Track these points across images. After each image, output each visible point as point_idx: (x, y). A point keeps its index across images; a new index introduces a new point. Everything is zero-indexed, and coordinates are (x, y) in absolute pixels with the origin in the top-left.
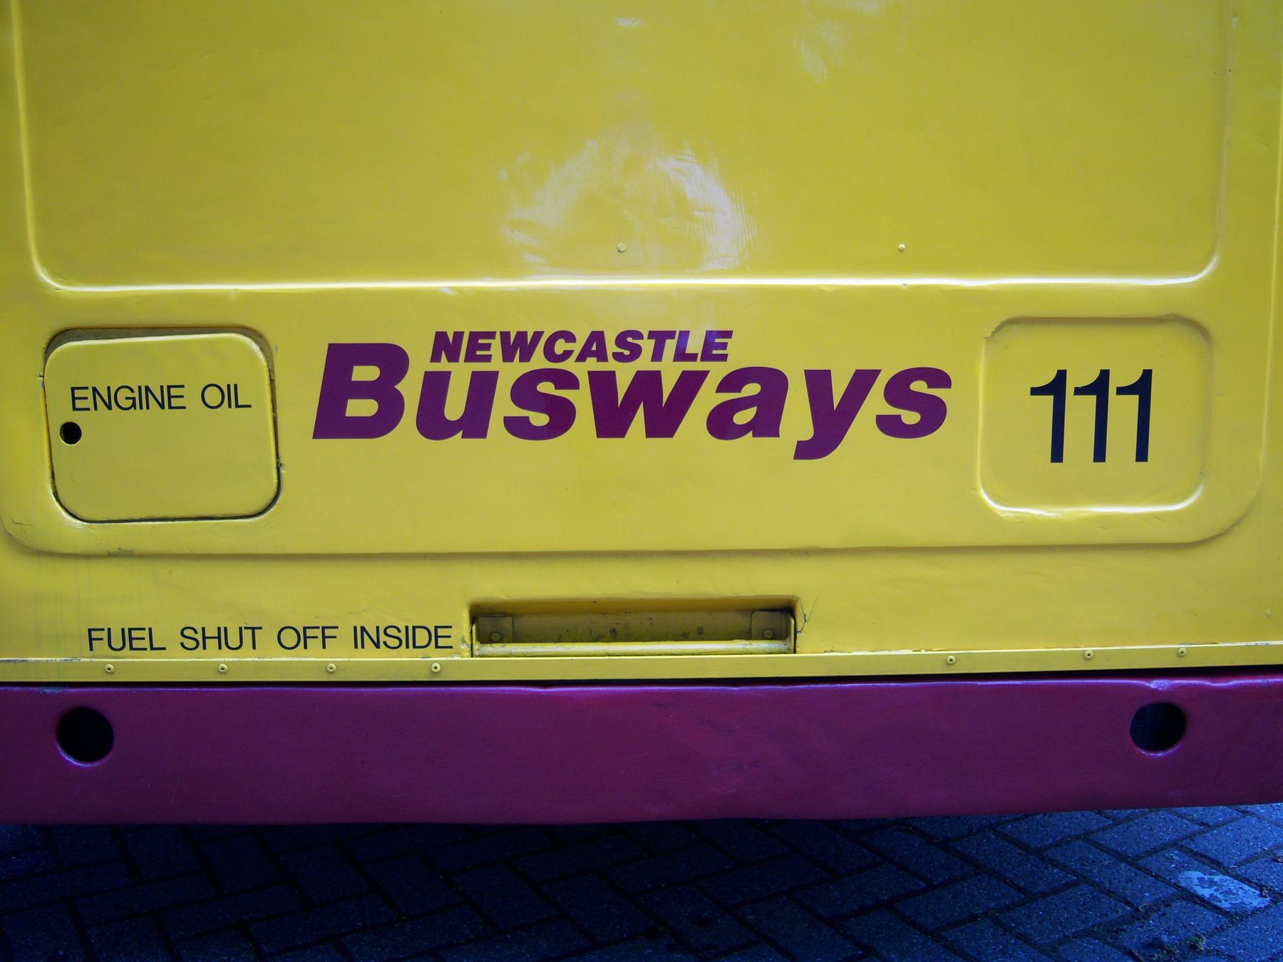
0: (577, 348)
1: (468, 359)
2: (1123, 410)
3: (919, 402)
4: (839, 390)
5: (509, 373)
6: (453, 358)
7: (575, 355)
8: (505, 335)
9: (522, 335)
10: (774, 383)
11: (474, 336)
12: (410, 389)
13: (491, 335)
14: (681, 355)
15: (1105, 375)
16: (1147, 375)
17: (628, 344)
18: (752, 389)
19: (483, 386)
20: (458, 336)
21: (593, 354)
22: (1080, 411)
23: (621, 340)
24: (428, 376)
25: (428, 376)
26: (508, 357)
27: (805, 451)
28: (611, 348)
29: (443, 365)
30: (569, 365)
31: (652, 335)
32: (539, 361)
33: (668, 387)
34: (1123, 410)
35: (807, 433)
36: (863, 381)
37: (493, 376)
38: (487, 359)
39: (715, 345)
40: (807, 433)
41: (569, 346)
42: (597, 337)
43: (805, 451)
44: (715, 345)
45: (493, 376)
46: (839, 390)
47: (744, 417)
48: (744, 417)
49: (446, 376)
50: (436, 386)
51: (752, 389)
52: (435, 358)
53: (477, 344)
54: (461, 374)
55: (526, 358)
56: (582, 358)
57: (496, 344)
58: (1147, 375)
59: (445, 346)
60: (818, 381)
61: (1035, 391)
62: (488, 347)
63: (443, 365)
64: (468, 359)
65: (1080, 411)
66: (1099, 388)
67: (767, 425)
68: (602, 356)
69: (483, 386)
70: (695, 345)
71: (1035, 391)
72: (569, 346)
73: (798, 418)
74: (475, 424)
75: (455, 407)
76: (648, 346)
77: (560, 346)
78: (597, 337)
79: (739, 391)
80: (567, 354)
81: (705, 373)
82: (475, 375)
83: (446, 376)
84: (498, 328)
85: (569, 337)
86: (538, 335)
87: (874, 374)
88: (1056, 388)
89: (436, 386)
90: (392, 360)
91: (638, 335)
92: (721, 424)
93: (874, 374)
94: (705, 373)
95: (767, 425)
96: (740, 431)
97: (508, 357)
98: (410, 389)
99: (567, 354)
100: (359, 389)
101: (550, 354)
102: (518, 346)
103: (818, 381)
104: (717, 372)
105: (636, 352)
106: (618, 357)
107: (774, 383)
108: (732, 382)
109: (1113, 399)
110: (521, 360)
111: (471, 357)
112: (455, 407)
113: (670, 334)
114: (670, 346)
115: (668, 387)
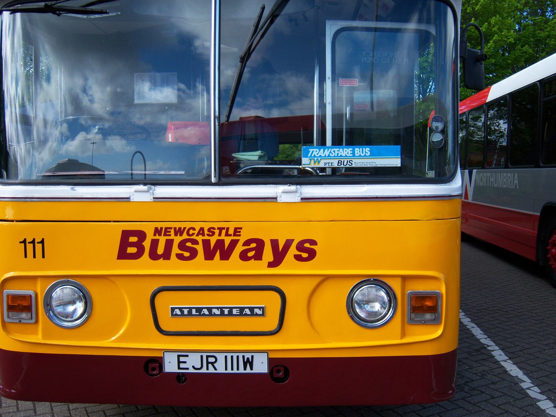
0: (196, 232)
1: (164, 235)
2: (39, 247)
5: (177, 240)
6: (160, 235)
7: (195, 235)
8: (175, 228)
9: (180, 228)
10: (260, 243)
11: (166, 228)
12: (147, 244)
13: (171, 228)
14: (227, 235)
15: (34, 239)
16: (43, 239)
17: (211, 231)
18: (253, 245)
19: (169, 243)
20: (161, 228)
21: (201, 234)
22: (30, 247)
23: (209, 230)
24: (152, 240)
25: (152, 240)
26: (176, 235)
28: (206, 232)
29: (157, 237)
30: (194, 237)
31: (218, 228)
32: (185, 236)
34: (39, 247)
35: (271, 259)
36: (288, 243)
37: (173, 240)
38: (170, 235)
39: (237, 231)
40: (271, 259)
41: (194, 232)
42: (202, 229)
43: (271, 265)
44: (237, 231)
45: (173, 240)
47: (251, 254)
48: (251, 254)
49: (158, 240)
50: (155, 243)
51: (253, 245)
52: (155, 235)
53: (167, 231)
54: (162, 240)
55: (181, 235)
56: (197, 235)
57: (172, 231)
58: (43, 239)
59: (157, 231)
60: (274, 243)
61: (20, 242)
62: (170, 232)
63: (157, 237)
64: (164, 235)
65: (30, 247)
66: (33, 242)
67: (258, 256)
68: (203, 235)
69: (169, 243)
70: (231, 232)
71: (20, 242)
72: (194, 232)
73: (268, 255)
74: (166, 255)
75: (160, 250)
76: (217, 232)
77: (191, 232)
78: (202, 229)
79: (249, 245)
80: (193, 234)
81: (238, 240)
82: (167, 240)
83: (158, 240)
84: (173, 227)
85: (194, 229)
86: (185, 228)
87: (293, 240)
88: (24, 242)
89: (155, 243)
90: (142, 235)
91: (214, 228)
92: (244, 256)
93: (293, 240)
94: (238, 240)
95: (258, 256)
96: (249, 259)
97: (176, 235)
98: (147, 244)
99: (193, 234)
101: (188, 234)
102: (178, 232)
103: (274, 243)
105: (213, 233)
106: (208, 235)
107: (260, 243)
109: (28, 245)
110: (180, 236)
111: (165, 235)
112: (160, 250)
113: (224, 228)
114: (224, 232)
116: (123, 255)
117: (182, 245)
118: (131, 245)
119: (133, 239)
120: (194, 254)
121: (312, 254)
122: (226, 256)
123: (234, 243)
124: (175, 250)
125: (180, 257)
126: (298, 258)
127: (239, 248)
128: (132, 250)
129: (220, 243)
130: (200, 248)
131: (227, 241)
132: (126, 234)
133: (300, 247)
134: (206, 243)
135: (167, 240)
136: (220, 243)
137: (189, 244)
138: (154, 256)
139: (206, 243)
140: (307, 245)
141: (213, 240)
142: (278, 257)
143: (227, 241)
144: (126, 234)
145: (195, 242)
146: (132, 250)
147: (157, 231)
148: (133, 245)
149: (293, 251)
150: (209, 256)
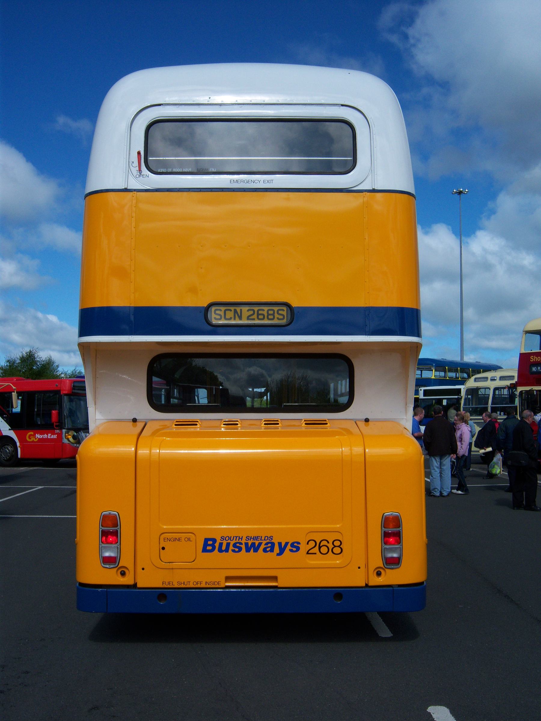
3: (295, 547)
4: (283, 545)
5: (232, 543)
10: (273, 544)
12: (217, 545)
18: (270, 545)
19: (228, 545)
24: (220, 543)
25: (220, 543)
27: (278, 555)
33: (256, 545)
35: (278, 552)
36: (287, 544)
43: (278, 555)
45: (230, 543)
46: (283, 545)
47: (268, 549)
50: (221, 545)
51: (270, 545)
54: (225, 543)
59: (223, 538)
60: (280, 544)
67: (272, 550)
69: (228, 545)
73: (277, 550)
74: (227, 550)
75: (224, 548)
89: (221, 545)
90: (214, 541)
95: (272, 550)
96: (268, 552)
98: (217, 545)
100: (209, 545)
103: (280, 544)
104: (264, 542)
108: (266, 544)
112: (224, 548)
115: (256, 545)
116: (205, 550)
117: (235, 545)
118: (209, 545)
119: (210, 542)
120: (240, 549)
121: (298, 549)
122: (256, 550)
123: (260, 544)
124: (231, 547)
125: (234, 551)
126: (291, 551)
127: (263, 546)
128: (209, 548)
129: (253, 544)
130: (243, 546)
131: (257, 543)
132: (206, 540)
133: (292, 545)
134: (246, 544)
135: (227, 543)
136: (253, 544)
137: (238, 545)
138: (220, 550)
139: (246, 544)
140: (295, 544)
141: (250, 543)
142: (282, 551)
143: (257, 543)
144: (206, 540)
145: (241, 544)
146: (209, 548)
147: (223, 538)
148: (210, 545)
149: (289, 547)
150: (248, 550)
